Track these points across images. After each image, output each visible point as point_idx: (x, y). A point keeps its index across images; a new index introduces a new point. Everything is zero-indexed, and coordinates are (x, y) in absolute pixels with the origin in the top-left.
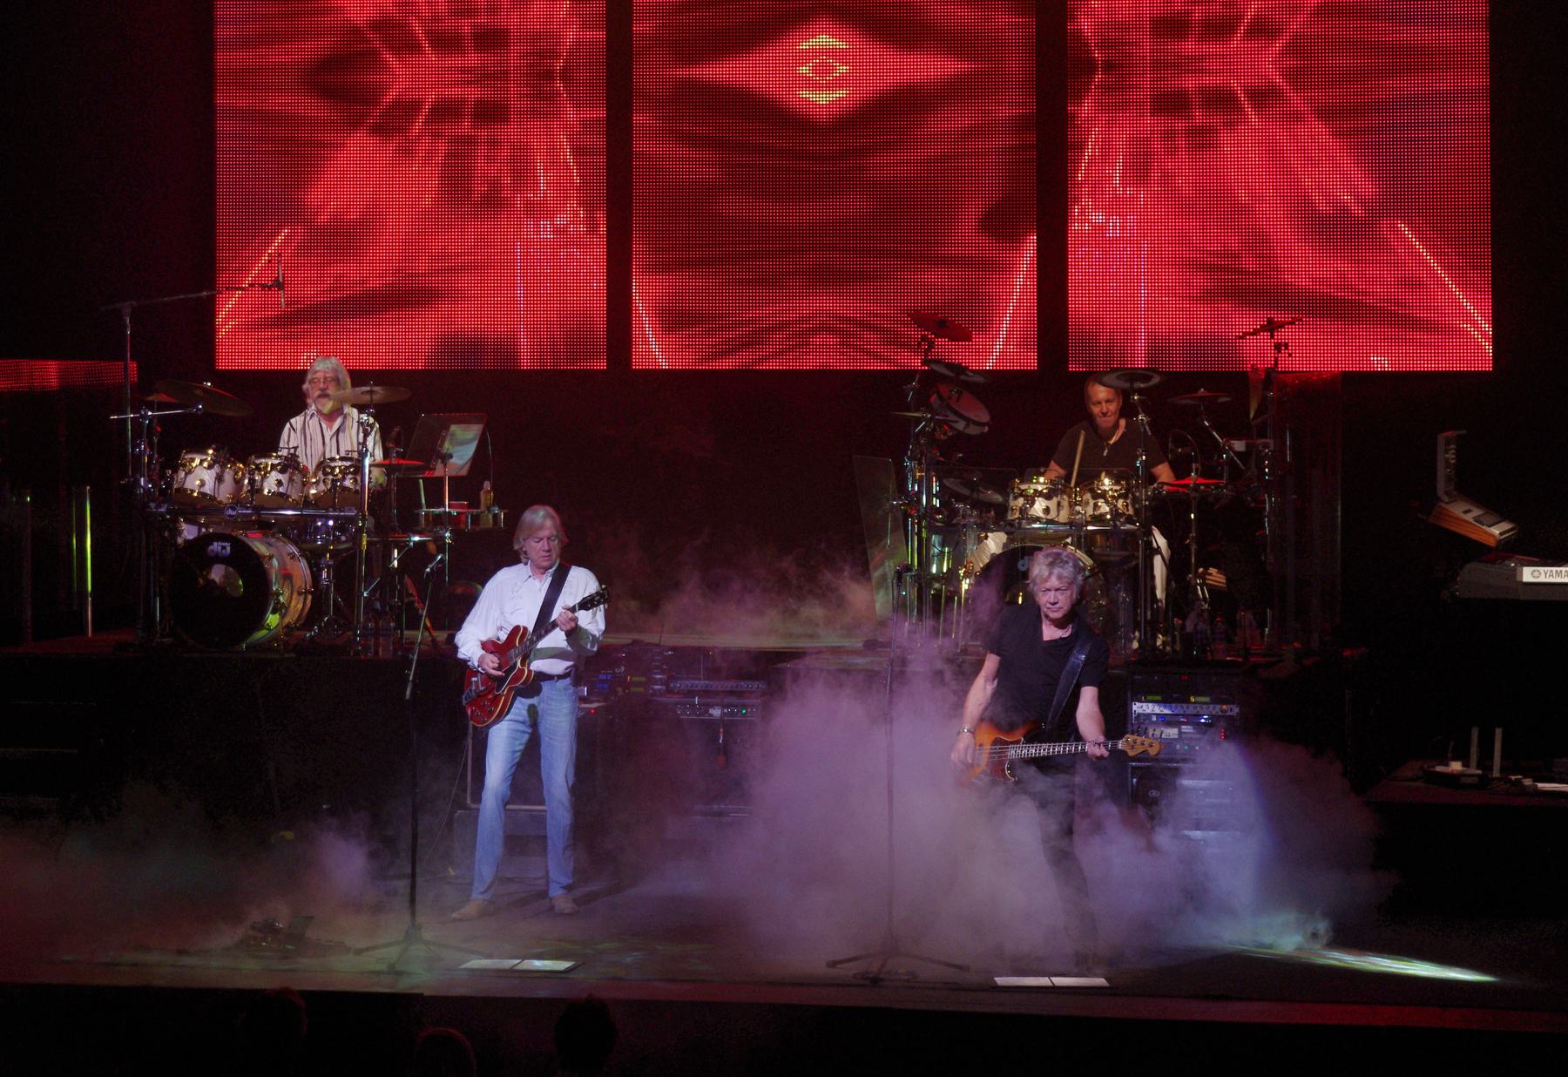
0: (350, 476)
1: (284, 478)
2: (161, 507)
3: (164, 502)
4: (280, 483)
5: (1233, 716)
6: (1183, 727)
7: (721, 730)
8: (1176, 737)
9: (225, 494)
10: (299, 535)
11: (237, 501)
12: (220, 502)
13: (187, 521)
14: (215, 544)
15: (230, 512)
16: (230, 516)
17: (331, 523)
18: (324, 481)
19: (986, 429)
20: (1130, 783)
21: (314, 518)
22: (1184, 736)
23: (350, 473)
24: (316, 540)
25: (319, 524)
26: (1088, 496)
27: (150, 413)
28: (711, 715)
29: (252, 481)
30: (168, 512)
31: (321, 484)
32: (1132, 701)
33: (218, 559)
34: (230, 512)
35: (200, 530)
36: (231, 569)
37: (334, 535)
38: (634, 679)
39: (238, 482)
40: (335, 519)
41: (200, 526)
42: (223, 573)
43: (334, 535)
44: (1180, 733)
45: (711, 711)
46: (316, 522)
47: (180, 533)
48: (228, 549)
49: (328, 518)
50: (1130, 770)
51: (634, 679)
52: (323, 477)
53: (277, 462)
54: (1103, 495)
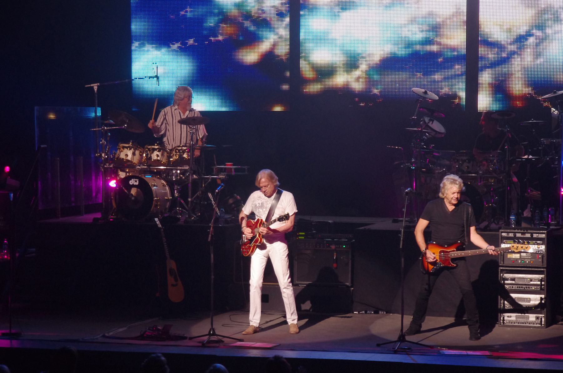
0: (186, 153)
1: (158, 153)
2: (110, 165)
3: (112, 163)
4: (158, 156)
5: (542, 250)
6: (522, 254)
7: (335, 254)
8: (519, 258)
9: (136, 160)
10: (166, 176)
11: (140, 163)
12: (134, 163)
13: (122, 171)
14: (132, 180)
15: (138, 167)
16: (138, 169)
17: (179, 172)
18: (176, 155)
19: (443, 136)
20: (499, 276)
21: (172, 169)
22: (522, 257)
23: (186, 152)
24: (173, 178)
25: (174, 172)
26: (484, 162)
27: (106, 128)
28: (331, 248)
29: (147, 155)
30: (114, 167)
31: (175, 156)
32: (501, 243)
33: (133, 186)
34: (138, 167)
35: (126, 174)
36: (139, 190)
37: (180, 176)
38: (300, 233)
39: (141, 156)
40: (180, 170)
41: (126, 172)
42: (136, 191)
43: (180, 176)
44: (521, 256)
45: (331, 246)
46: (172, 171)
47: (118, 175)
48: (138, 182)
49: (177, 170)
50: (500, 270)
51: (300, 233)
52: (175, 154)
53: (157, 147)
54: (492, 161)
